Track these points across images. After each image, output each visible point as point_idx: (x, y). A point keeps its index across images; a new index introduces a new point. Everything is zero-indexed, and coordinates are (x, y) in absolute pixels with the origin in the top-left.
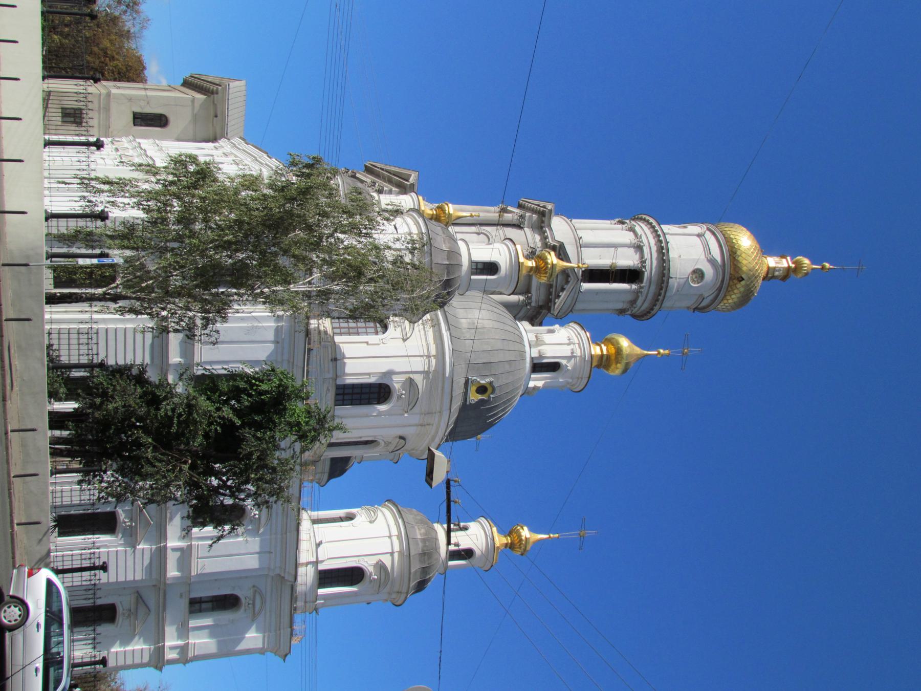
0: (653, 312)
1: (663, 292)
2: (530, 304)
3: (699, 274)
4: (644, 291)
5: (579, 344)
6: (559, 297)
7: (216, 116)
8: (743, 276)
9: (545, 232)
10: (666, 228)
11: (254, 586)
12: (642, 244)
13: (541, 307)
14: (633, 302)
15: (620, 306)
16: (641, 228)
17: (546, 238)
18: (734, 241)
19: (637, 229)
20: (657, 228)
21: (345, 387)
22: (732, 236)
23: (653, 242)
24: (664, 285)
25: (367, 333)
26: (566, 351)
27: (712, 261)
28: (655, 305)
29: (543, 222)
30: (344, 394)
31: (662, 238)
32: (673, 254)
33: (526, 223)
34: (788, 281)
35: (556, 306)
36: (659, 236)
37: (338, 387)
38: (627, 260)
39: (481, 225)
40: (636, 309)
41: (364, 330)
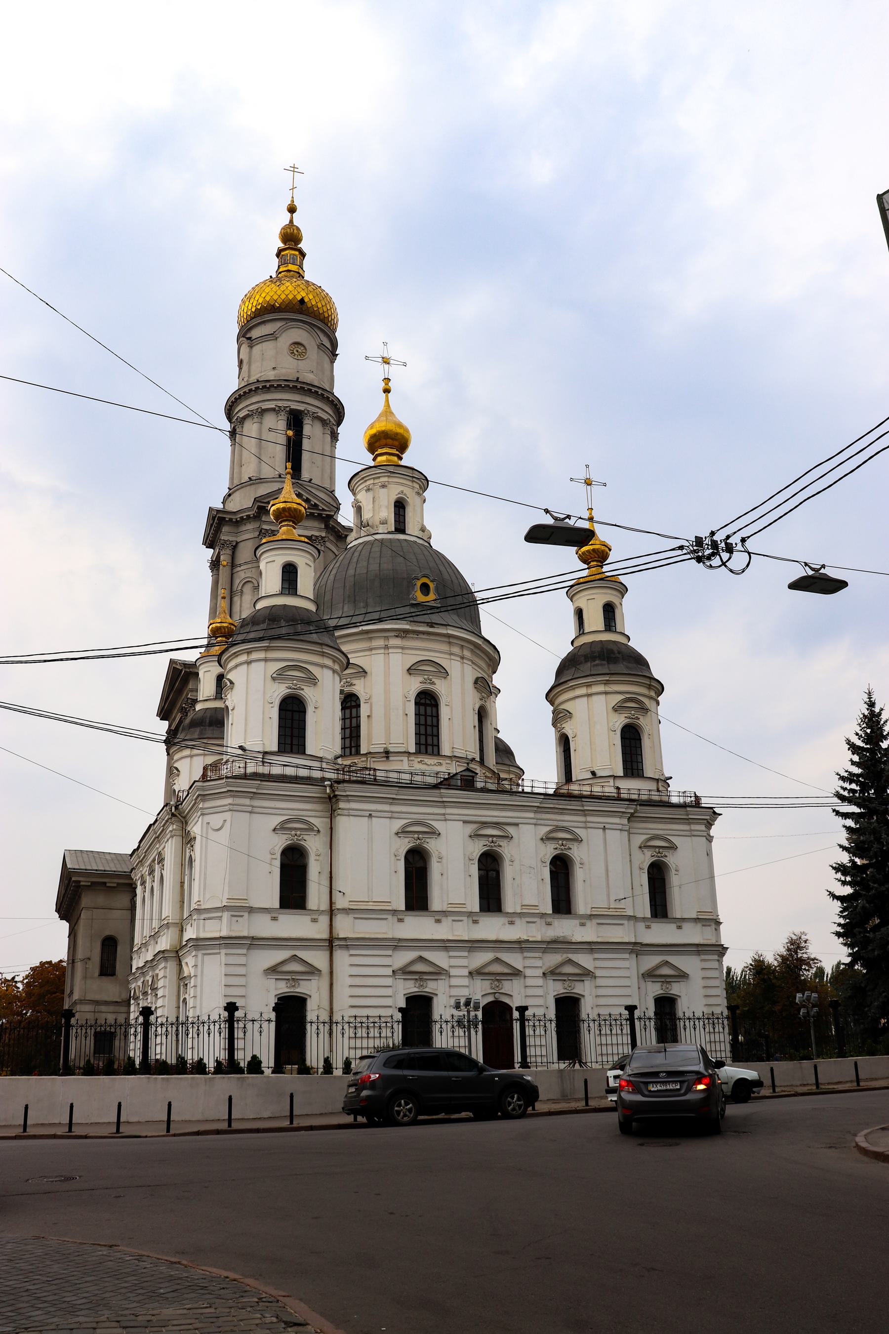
0: (336, 402)
1: (314, 389)
2: (322, 538)
5: (374, 479)
6: (316, 505)
7: (105, 883)
8: (299, 298)
9: (242, 518)
11: (640, 847)
12: (259, 410)
13: (327, 527)
14: (324, 422)
15: (328, 438)
17: (248, 516)
18: (259, 307)
19: (242, 414)
21: (418, 744)
22: (253, 310)
23: (254, 399)
24: (306, 387)
25: (358, 717)
28: (328, 398)
29: (231, 520)
30: (426, 745)
31: (253, 388)
33: (231, 539)
34: (305, 250)
36: (250, 390)
37: (418, 752)
40: (332, 420)
41: (354, 721)
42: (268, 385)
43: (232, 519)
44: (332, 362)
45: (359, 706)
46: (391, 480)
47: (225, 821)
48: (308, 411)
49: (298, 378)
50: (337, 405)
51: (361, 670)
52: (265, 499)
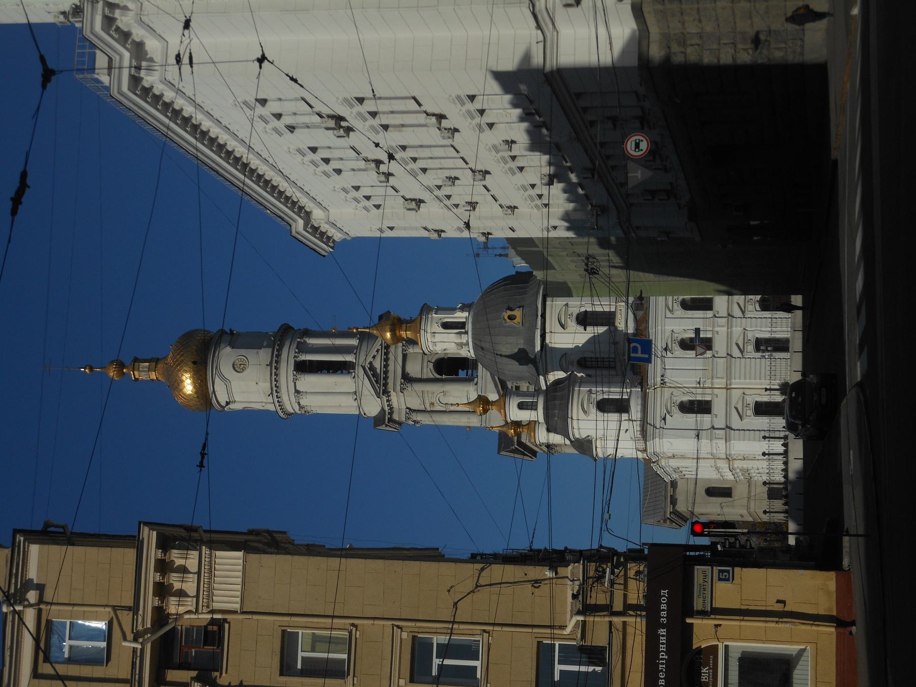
3: (238, 368)
4: (292, 354)
6: (378, 351)
7: (671, 495)
9: (388, 406)
10: (271, 408)
16: (290, 405)
17: (388, 401)
20: (279, 408)
23: (285, 398)
26: (438, 338)
27: (224, 379)
32: (266, 386)
35: (380, 343)
38: (309, 382)
39: (445, 412)
42: (275, 389)
43: (389, 412)
44: (239, 334)
45: (585, 358)
46: (429, 331)
47: (667, 441)
48: (295, 357)
49: (268, 365)
50: (282, 332)
51: (564, 356)
52: (377, 391)
